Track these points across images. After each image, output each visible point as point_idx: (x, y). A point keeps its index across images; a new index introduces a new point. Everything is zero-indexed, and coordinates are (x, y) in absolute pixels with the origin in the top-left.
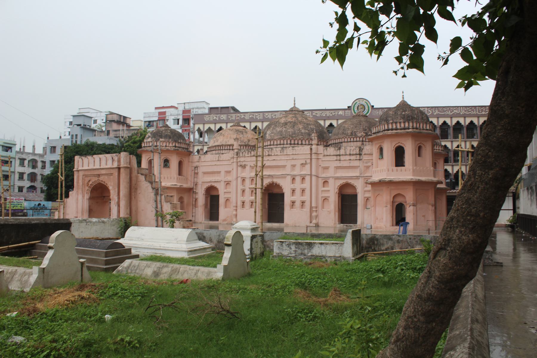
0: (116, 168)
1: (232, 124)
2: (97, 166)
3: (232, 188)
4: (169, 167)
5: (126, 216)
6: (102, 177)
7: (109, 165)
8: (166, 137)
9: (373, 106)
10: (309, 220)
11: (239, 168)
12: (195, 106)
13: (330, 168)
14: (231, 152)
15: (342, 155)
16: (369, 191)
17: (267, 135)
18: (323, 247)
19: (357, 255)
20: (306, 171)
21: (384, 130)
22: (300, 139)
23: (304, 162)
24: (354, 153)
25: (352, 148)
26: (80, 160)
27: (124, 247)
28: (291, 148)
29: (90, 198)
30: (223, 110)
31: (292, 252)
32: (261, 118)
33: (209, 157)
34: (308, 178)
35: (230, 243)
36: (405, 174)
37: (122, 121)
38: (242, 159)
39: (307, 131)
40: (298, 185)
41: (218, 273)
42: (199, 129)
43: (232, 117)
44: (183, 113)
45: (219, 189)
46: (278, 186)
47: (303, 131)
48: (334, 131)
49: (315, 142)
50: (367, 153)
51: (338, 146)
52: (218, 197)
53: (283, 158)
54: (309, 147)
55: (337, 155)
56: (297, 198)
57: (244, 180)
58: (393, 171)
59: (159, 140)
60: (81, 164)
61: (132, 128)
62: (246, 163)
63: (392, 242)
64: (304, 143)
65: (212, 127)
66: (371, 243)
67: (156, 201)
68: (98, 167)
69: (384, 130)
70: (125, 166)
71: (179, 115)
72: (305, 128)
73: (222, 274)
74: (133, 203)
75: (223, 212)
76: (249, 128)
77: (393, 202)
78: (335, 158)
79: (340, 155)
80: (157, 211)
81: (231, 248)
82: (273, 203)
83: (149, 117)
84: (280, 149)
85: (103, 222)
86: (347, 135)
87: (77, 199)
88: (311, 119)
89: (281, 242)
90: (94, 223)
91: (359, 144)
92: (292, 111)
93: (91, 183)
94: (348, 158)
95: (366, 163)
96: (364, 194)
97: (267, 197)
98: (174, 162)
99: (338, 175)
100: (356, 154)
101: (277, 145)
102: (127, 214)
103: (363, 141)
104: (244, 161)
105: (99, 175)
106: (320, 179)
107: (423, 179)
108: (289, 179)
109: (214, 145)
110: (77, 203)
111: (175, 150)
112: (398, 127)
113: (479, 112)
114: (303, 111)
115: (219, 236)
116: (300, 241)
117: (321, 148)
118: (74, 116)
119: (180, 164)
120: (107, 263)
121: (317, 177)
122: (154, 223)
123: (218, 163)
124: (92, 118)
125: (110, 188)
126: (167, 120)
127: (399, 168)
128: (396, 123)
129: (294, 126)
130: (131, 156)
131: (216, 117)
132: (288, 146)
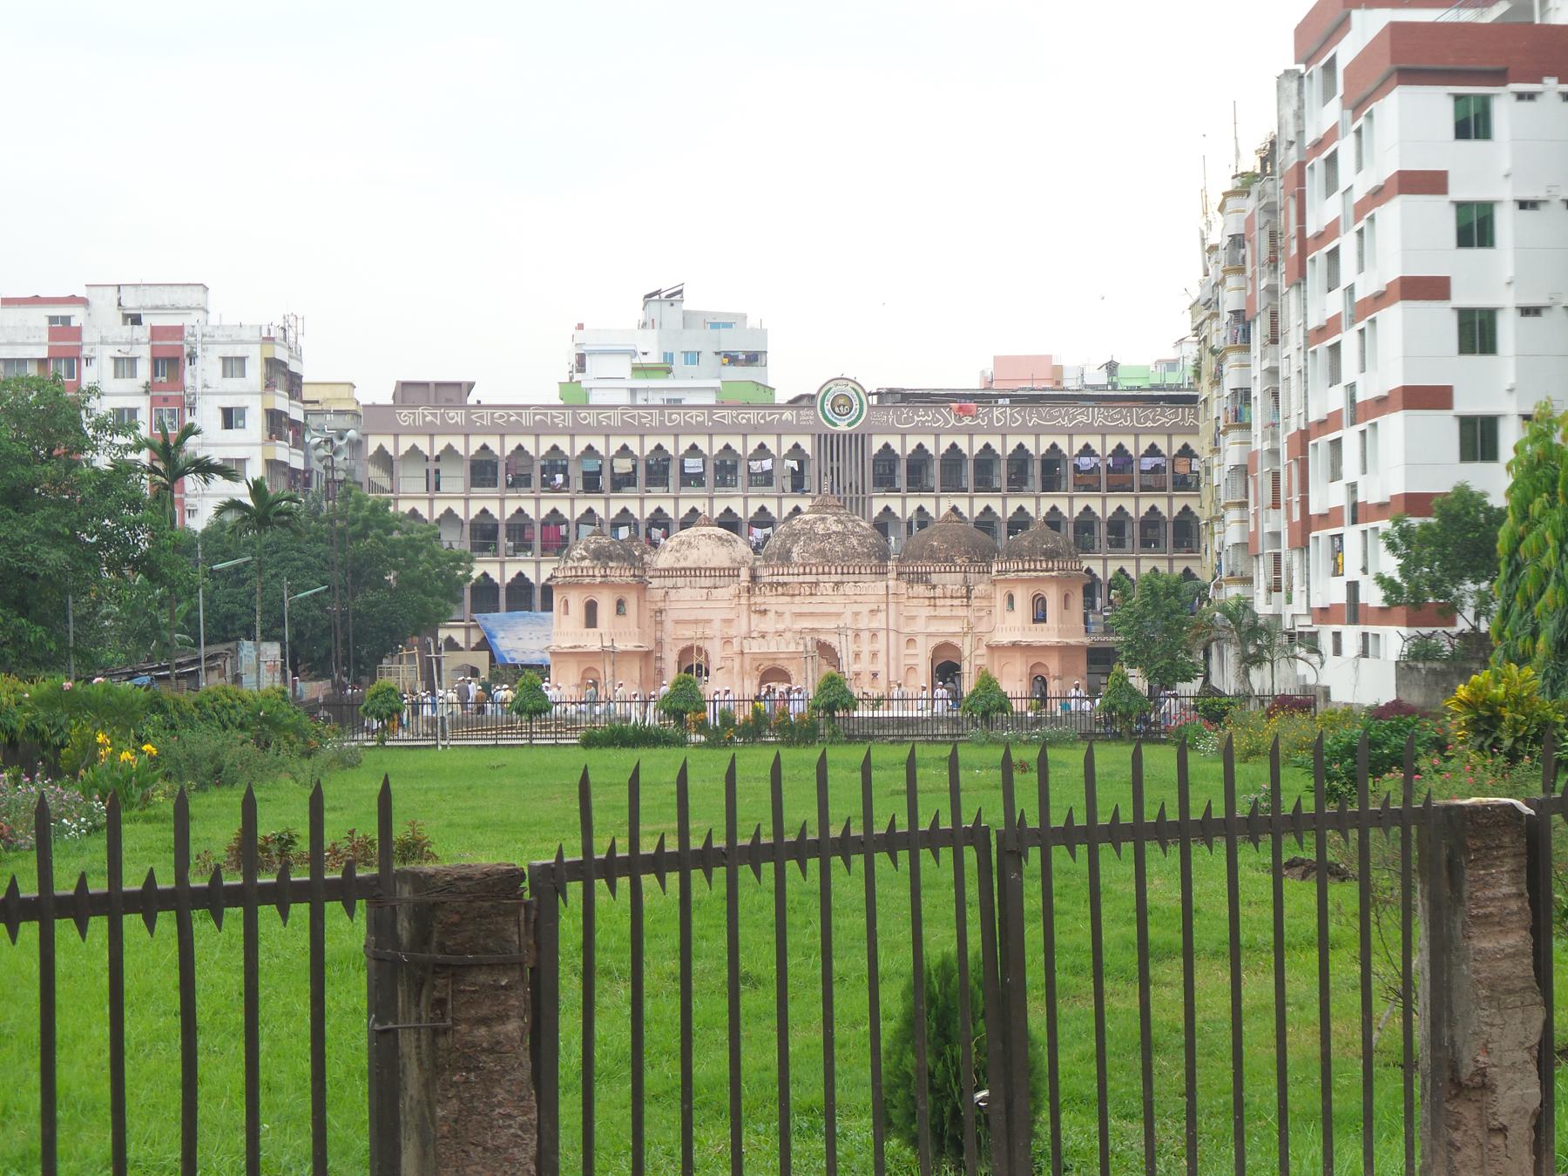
7: (792, 648)
12: (166, 298)
20: (878, 622)
32: (569, 423)
34: (882, 635)
36: (1048, 634)
38: (759, 600)
43: (481, 417)
49: (893, 575)
53: (840, 599)
56: (864, 666)
65: (423, 444)
71: (138, 342)
78: (927, 602)
94: (948, 602)
99: (932, 629)
107: (1072, 641)
123: (707, 605)
126: (89, 360)
131: (435, 415)
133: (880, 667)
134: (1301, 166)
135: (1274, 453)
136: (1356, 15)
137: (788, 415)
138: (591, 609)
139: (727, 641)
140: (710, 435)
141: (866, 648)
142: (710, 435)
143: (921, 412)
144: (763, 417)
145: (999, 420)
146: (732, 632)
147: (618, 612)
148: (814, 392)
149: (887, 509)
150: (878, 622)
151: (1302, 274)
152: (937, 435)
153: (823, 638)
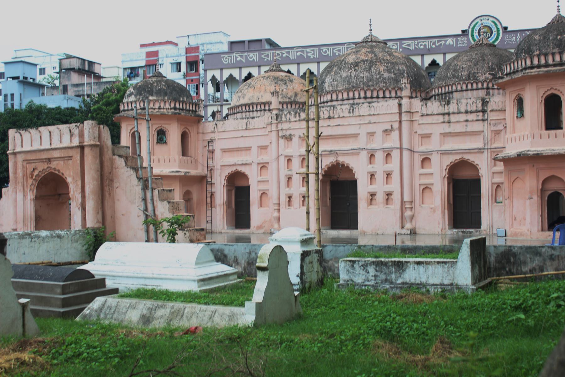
0: (77, 147)
1: (267, 68)
2: (46, 146)
3: (271, 174)
4: (166, 143)
5: (97, 226)
6: (55, 163)
7: (66, 143)
8: (159, 92)
9: (506, 28)
10: (399, 224)
11: (282, 141)
12: (207, 39)
13: (432, 137)
14: (268, 114)
15: (454, 113)
16: (502, 173)
17: (326, 85)
18: (421, 268)
19: (480, 281)
20: (393, 141)
21: (526, 69)
22: (381, 89)
23: (390, 128)
24: (474, 109)
25: (470, 102)
26: (18, 135)
27: (93, 276)
28: (366, 105)
29: (37, 199)
30: (251, 44)
31: (370, 278)
32: (317, 55)
33: (231, 123)
34: (395, 154)
35: (265, 265)
37: (87, 69)
38: (285, 126)
39: (392, 76)
40: (380, 166)
41: (246, 316)
42: (214, 77)
43: (267, 56)
44: (187, 53)
45: (249, 177)
46: (346, 169)
47: (386, 75)
48: (439, 72)
49: (406, 92)
50: (495, 108)
51: (446, 98)
52: (247, 189)
53: (353, 121)
54: (397, 101)
55: (444, 114)
56: (379, 187)
57: (289, 161)
58: (541, 138)
59: (147, 98)
60: (18, 142)
61: (103, 80)
62: (292, 132)
63: (541, 259)
64: (387, 95)
65: (235, 73)
66: (504, 261)
67: (145, 199)
68: (48, 147)
69: (526, 69)
70: (92, 143)
71: (181, 56)
72: (388, 70)
73: (254, 317)
74: (107, 204)
75: (257, 214)
76: (296, 74)
77: (543, 190)
78: (441, 118)
79: (449, 114)
80: (147, 216)
81: (267, 273)
82: (339, 196)
83: (131, 61)
84: (348, 106)
85: (59, 236)
86: (461, 79)
87: (16, 201)
88: (400, 55)
89: (350, 261)
90: (44, 238)
91: (482, 93)
92: (367, 42)
93: (36, 173)
94: (463, 117)
95: (495, 125)
96: (492, 178)
97: (328, 188)
98: (174, 134)
99: (446, 147)
100: (477, 111)
101: (343, 100)
102: (98, 222)
103: (488, 88)
104: (289, 129)
105: (49, 160)
106: (416, 155)
108: (364, 155)
109: (238, 104)
110: (16, 207)
111: (176, 114)
112: (550, 61)
114: (385, 42)
115: (250, 253)
116: (383, 259)
117: (417, 103)
118: (6, 63)
119: (184, 137)
120: (65, 303)
121: (411, 151)
122: (143, 235)
123: (246, 133)
124: (36, 65)
125: (69, 180)
126: (161, 65)
127: (552, 132)
128: (546, 55)
129: (370, 68)
130: (102, 126)
131: (242, 56)
132: (362, 101)
137: (450, 41)
146: (265, 158)
150: (393, 141)
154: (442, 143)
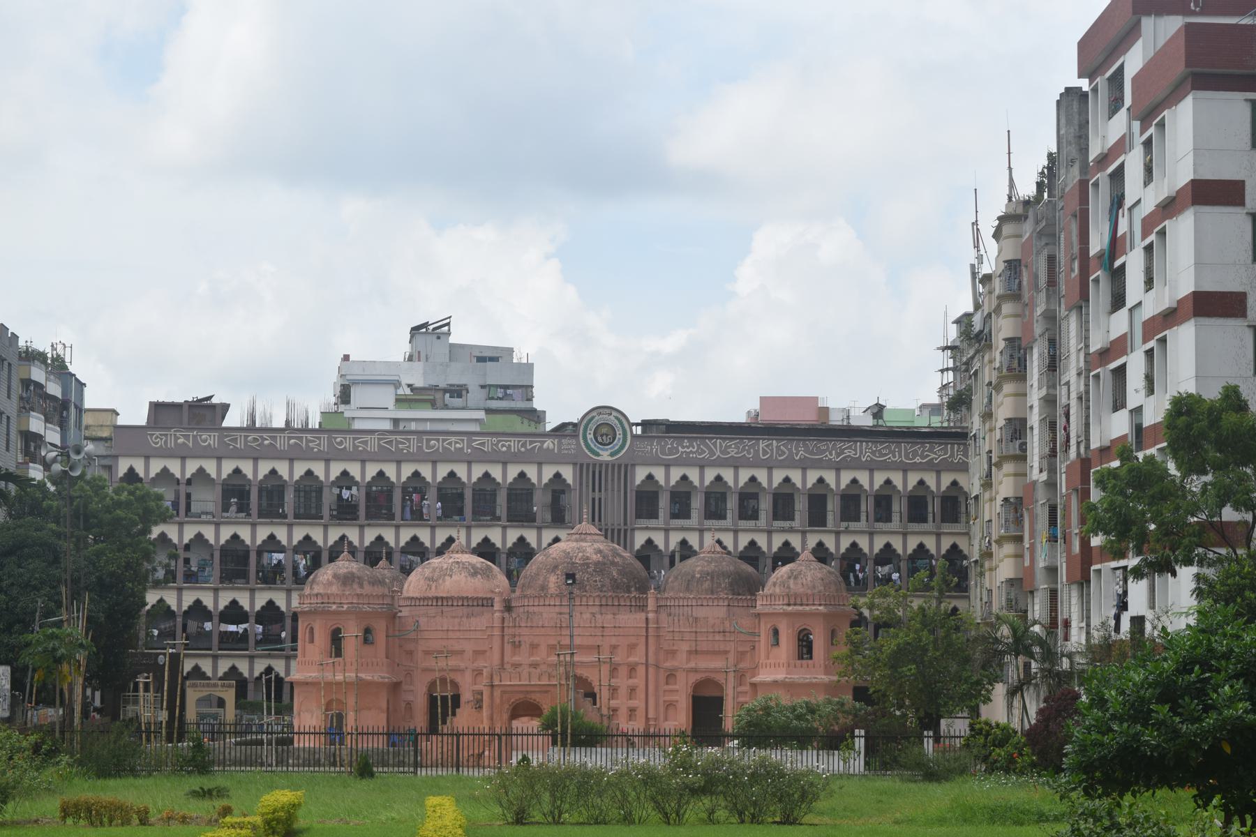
11: (508, 647)
17: (552, 585)
20: (638, 657)
32: (324, 446)
34: (641, 670)
42: (131, 470)
43: (235, 440)
54: (643, 615)
65: (174, 467)
72: (620, 572)
99: (692, 665)
108: (605, 670)
113: (907, 457)
121: (657, 667)
131: (187, 437)
133: (638, 703)
134: (1083, 185)
135: (1051, 485)
136: (1147, 23)
137: (548, 443)
138: (336, 639)
139: (478, 673)
140: (469, 463)
141: (622, 682)
142: (469, 463)
143: (686, 443)
144: (524, 445)
145: (765, 453)
147: (366, 641)
148: (576, 421)
149: (649, 542)
151: (1085, 296)
152: (702, 468)
153: (579, 672)
154: (688, 660)
